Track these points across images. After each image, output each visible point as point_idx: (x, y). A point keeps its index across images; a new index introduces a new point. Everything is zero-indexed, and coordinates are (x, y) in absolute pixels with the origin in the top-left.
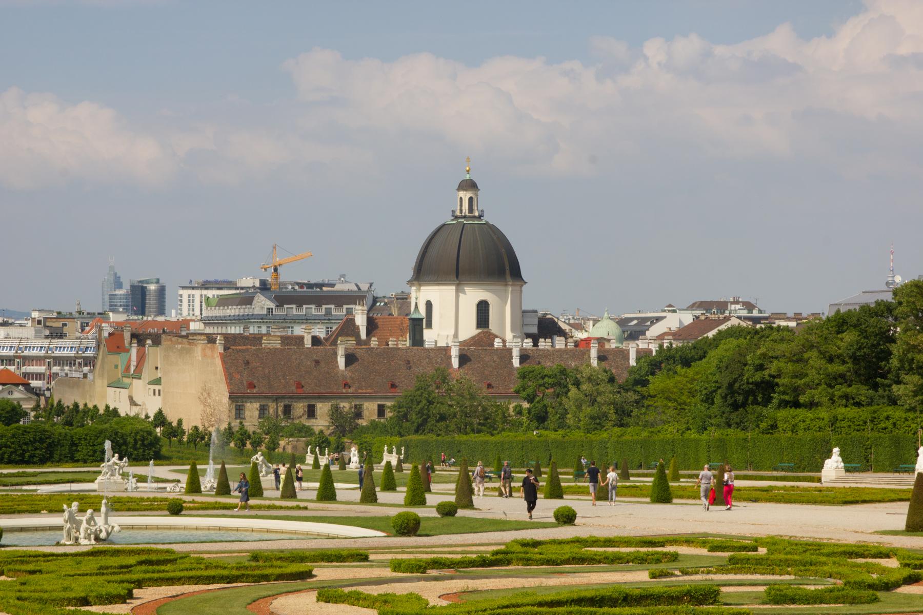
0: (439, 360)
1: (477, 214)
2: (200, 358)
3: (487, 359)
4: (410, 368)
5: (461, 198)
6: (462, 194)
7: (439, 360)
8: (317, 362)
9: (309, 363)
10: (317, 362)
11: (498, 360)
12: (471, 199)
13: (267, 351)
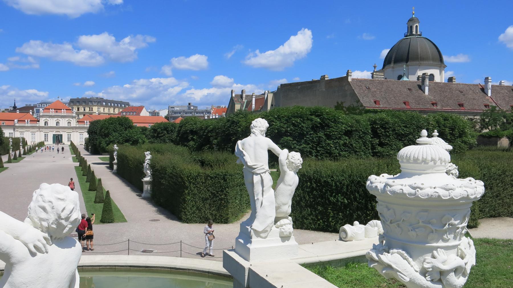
0: (477, 91)
1: (418, 33)
2: (324, 90)
3: (502, 91)
4: (464, 95)
5: (411, 27)
6: (411, 24)
7: (477, 91)
8: (409, 89)
9: (405, 90)
10: (409, 89)
11: (508, 92)
12: (417, 26)
13: (378, 82)
